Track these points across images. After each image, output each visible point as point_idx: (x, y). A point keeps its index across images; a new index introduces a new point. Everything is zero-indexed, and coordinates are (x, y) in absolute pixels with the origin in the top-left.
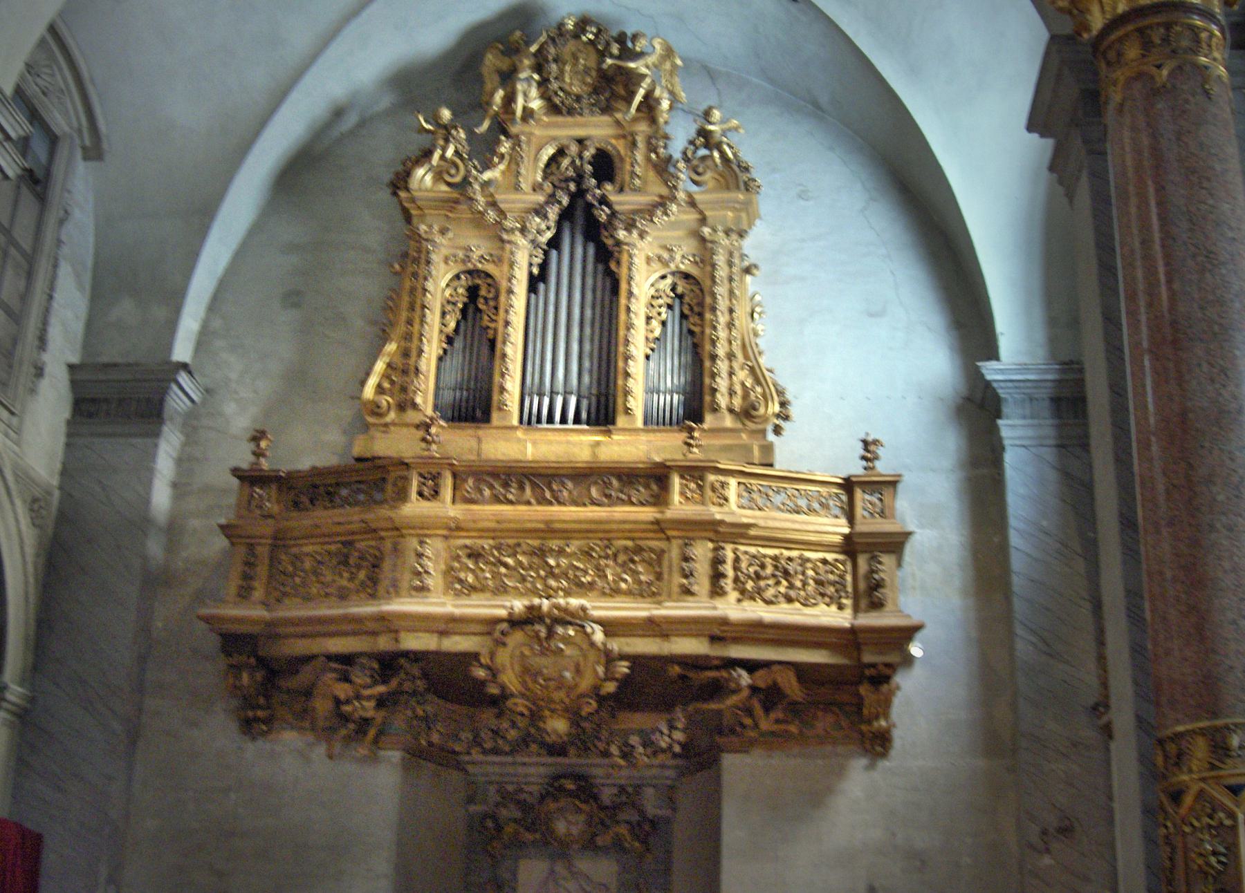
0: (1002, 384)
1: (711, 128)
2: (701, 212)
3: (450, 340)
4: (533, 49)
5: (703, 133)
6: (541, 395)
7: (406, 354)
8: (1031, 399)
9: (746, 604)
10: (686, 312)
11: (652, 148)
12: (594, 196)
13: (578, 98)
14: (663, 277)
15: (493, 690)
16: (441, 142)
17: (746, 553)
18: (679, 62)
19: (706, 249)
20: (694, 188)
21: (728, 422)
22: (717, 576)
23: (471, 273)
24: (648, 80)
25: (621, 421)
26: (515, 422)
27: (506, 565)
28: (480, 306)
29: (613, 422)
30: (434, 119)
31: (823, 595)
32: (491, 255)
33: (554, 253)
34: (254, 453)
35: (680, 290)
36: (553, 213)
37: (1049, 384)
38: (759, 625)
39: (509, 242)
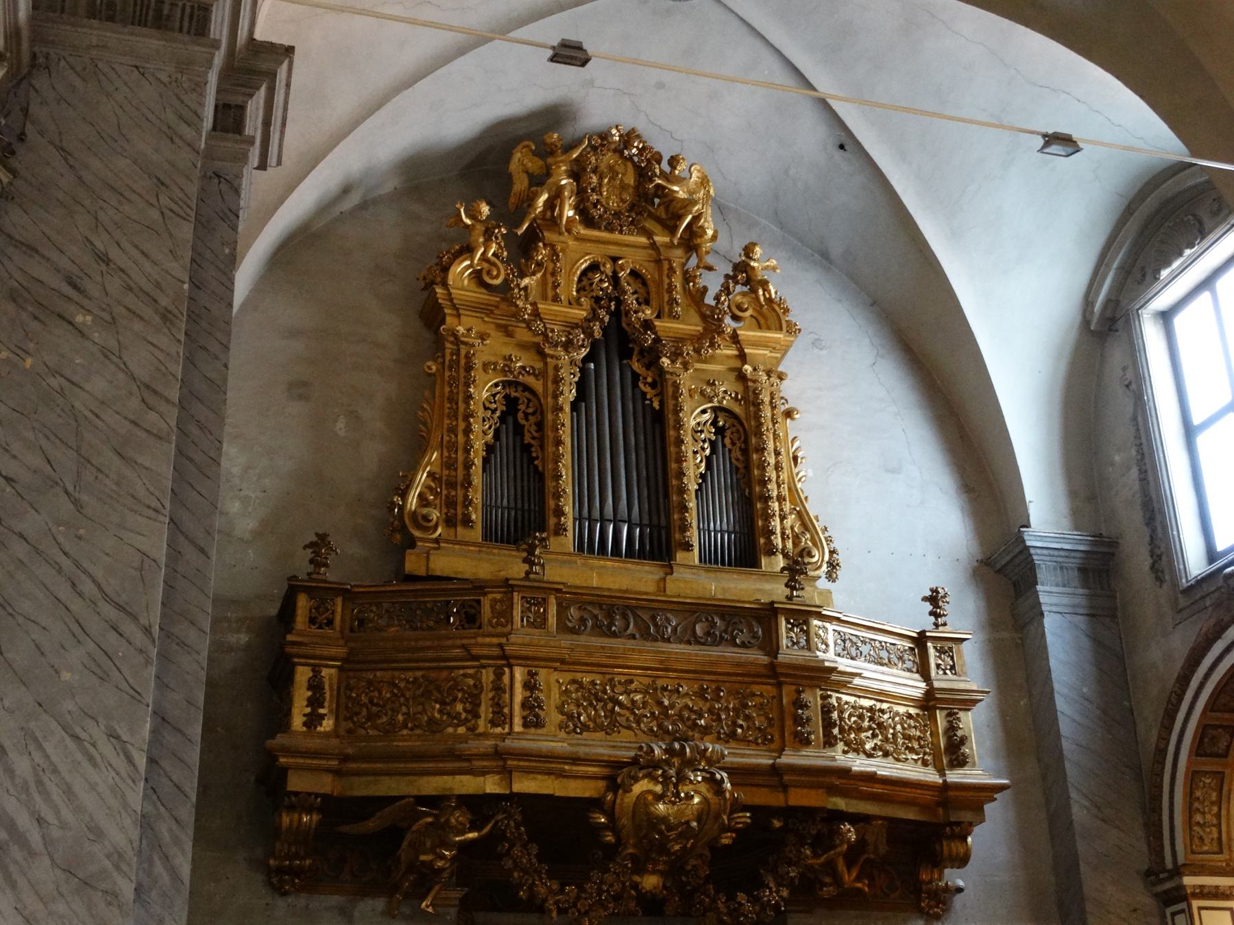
0: (1039, 551)
1: (753, 264)
7: (449, 464)
8: (1061, 568)
13: (617, 214)
14: (704, 412)
15: (610, 838)
17: (847, 703)
20: (734, 324)
22: (828, 724)
23: (506, 384)
25: (680, 556)
28: (523, 422)
31: (912, 750)
37: (1078, 555)
39: (552, 357)
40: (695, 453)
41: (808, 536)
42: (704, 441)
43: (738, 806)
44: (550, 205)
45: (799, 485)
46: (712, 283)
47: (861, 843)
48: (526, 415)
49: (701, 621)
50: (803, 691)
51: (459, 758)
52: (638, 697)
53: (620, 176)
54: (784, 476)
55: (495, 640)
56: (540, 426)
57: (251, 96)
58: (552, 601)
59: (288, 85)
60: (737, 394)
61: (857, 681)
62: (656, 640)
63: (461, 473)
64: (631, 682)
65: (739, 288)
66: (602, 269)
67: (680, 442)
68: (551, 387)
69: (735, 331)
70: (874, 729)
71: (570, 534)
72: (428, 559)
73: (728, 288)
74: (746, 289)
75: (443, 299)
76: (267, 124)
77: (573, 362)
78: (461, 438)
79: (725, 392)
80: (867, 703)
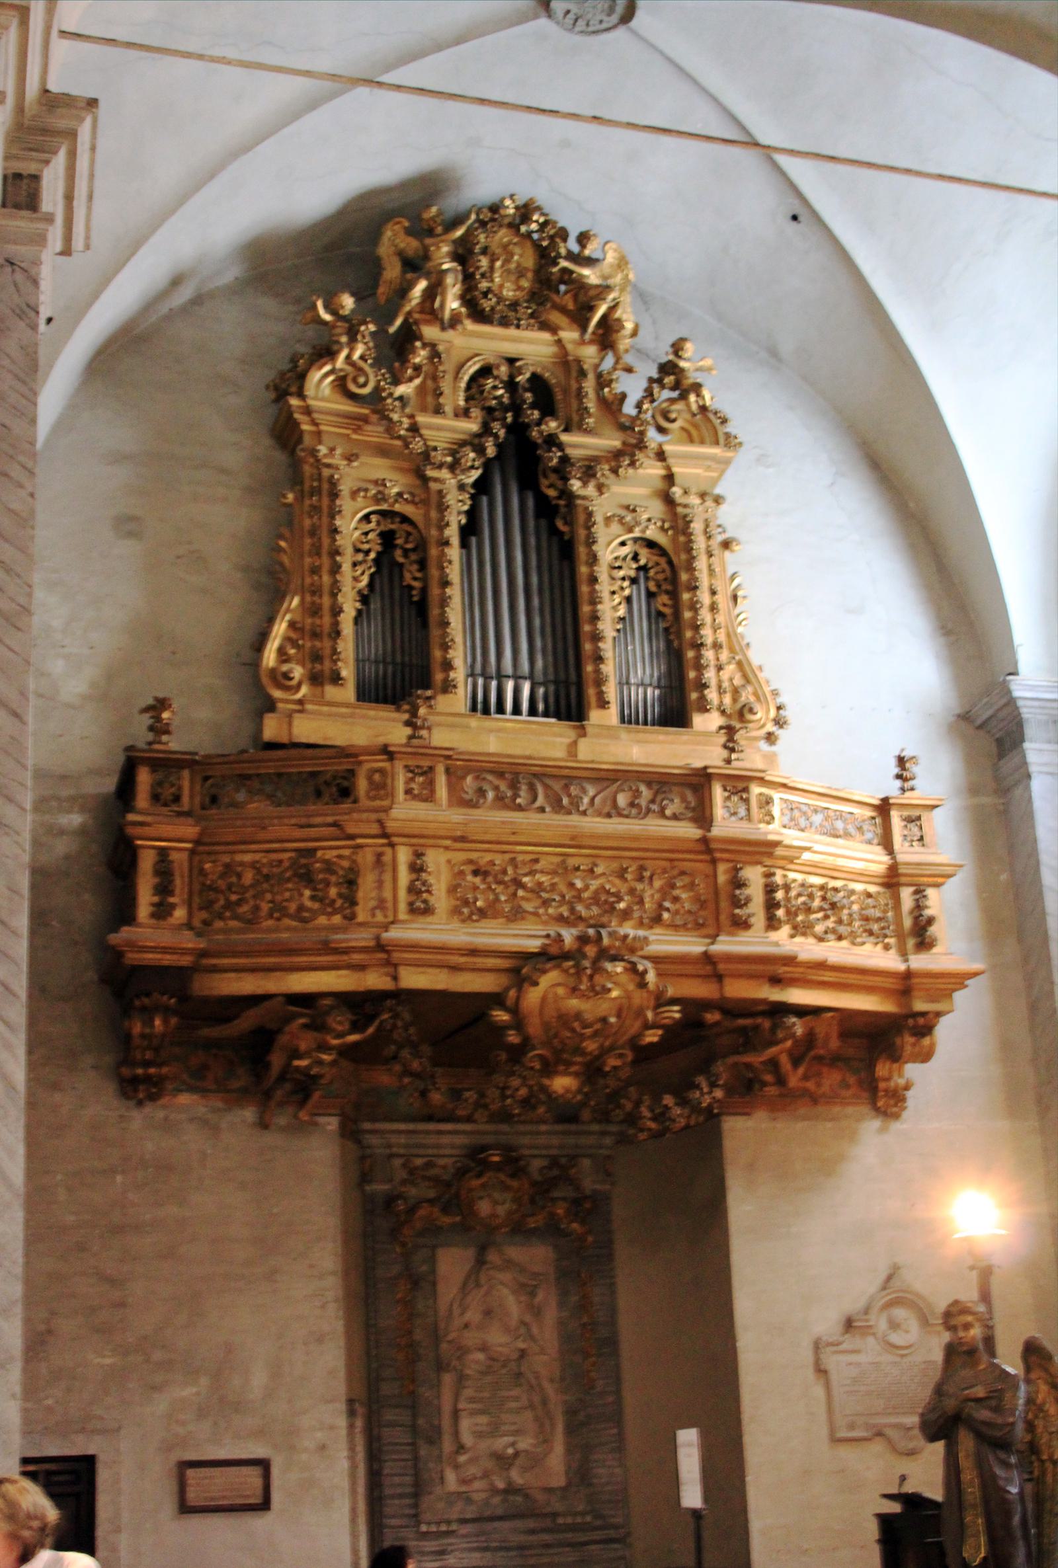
1: (682, 364)
2: (668, 468)
3: (364, 599)
4: (459, 233)
5: (668, 368)
9: (798, 939)
10: (653, 588)
13: (514, 305)
14: (623, 544)
17: (794, 881)
19: (675, 514)
22: (771, 905)
25: (595, 716)
33: (484, 499)
34: (151, 728)
39: (436, 480)
40: (613, 593)
42: (623, 579)
43: (661, 1001)
44: (431, 294)
45: (740, 630)
46: (632, 387)
47: (810, 1039)
48: (406, 552)
51: (337, 951)
52: (543, 878)
54: (720, 619)
55: (374, 816)
56: (423, 565)
57: (47, 162)
58: (440, 769)
59: (93, 149)
61: (806, 856)
63: (327, 620)
64: (536, 861)
65: (666, 394)
66: (495, 372)
67: (593, 580)
68: (434, 514)
69: (660, 445)
71: (461, 690)
72: (290, 724)
73: (651, 394)
74: (675, 394)
76: (69, 198)
77: (461, 487)
78: (326, 579)
79: (649, 520)
80: (817, 881)
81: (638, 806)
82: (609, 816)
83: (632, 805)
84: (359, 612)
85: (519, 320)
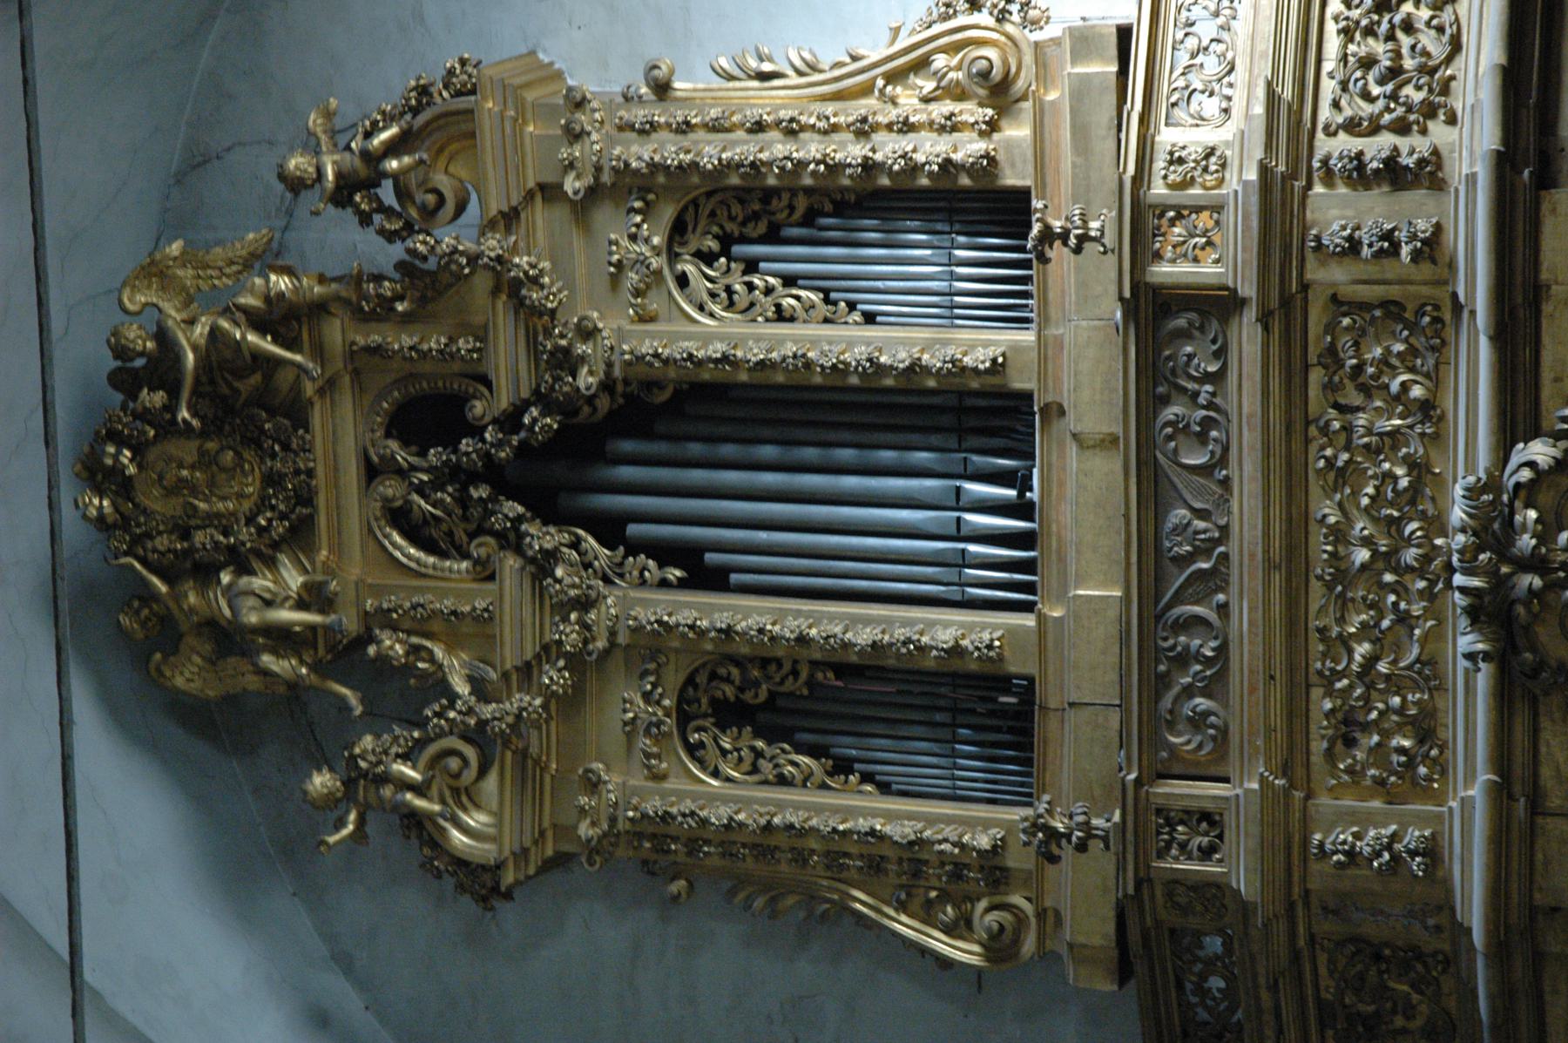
2: (530, 196)
3: (842, 767)
6: (964, 561)
7: (875, 866)
10: (762, 228)
11: (383, 311)
12: (499, 445)
13: (272, 480)
14: (682, 281)
16: (387, 791)
17: (1336, 105)
18: (175, 248)
21: (1017, 132)
23: (684, 719)
24: (225, 324)
26: (1029, 621)
27: (1371, 661)
28: (763, 695)
29: (1027, 396)
30: (332, 807)
32: (644, 674)
33: (633, 529)
35: (712, 244)
36: (542, 537)
38: (1512, 78)
39: (613, 633)
41: (940, 61)
49: (1176, 450)
50: (1318, 238)
53: (185, 473)
60: (637, 211)
62: (1225, 557)
66: (398, 503)
70: (1393, 27)
75: (527, 864)
80: (1333, 44)
81: (1207, 423)
82: (1225, 483)
83: (1202, 438)
84: (867, 778)
85: (297, 472)
